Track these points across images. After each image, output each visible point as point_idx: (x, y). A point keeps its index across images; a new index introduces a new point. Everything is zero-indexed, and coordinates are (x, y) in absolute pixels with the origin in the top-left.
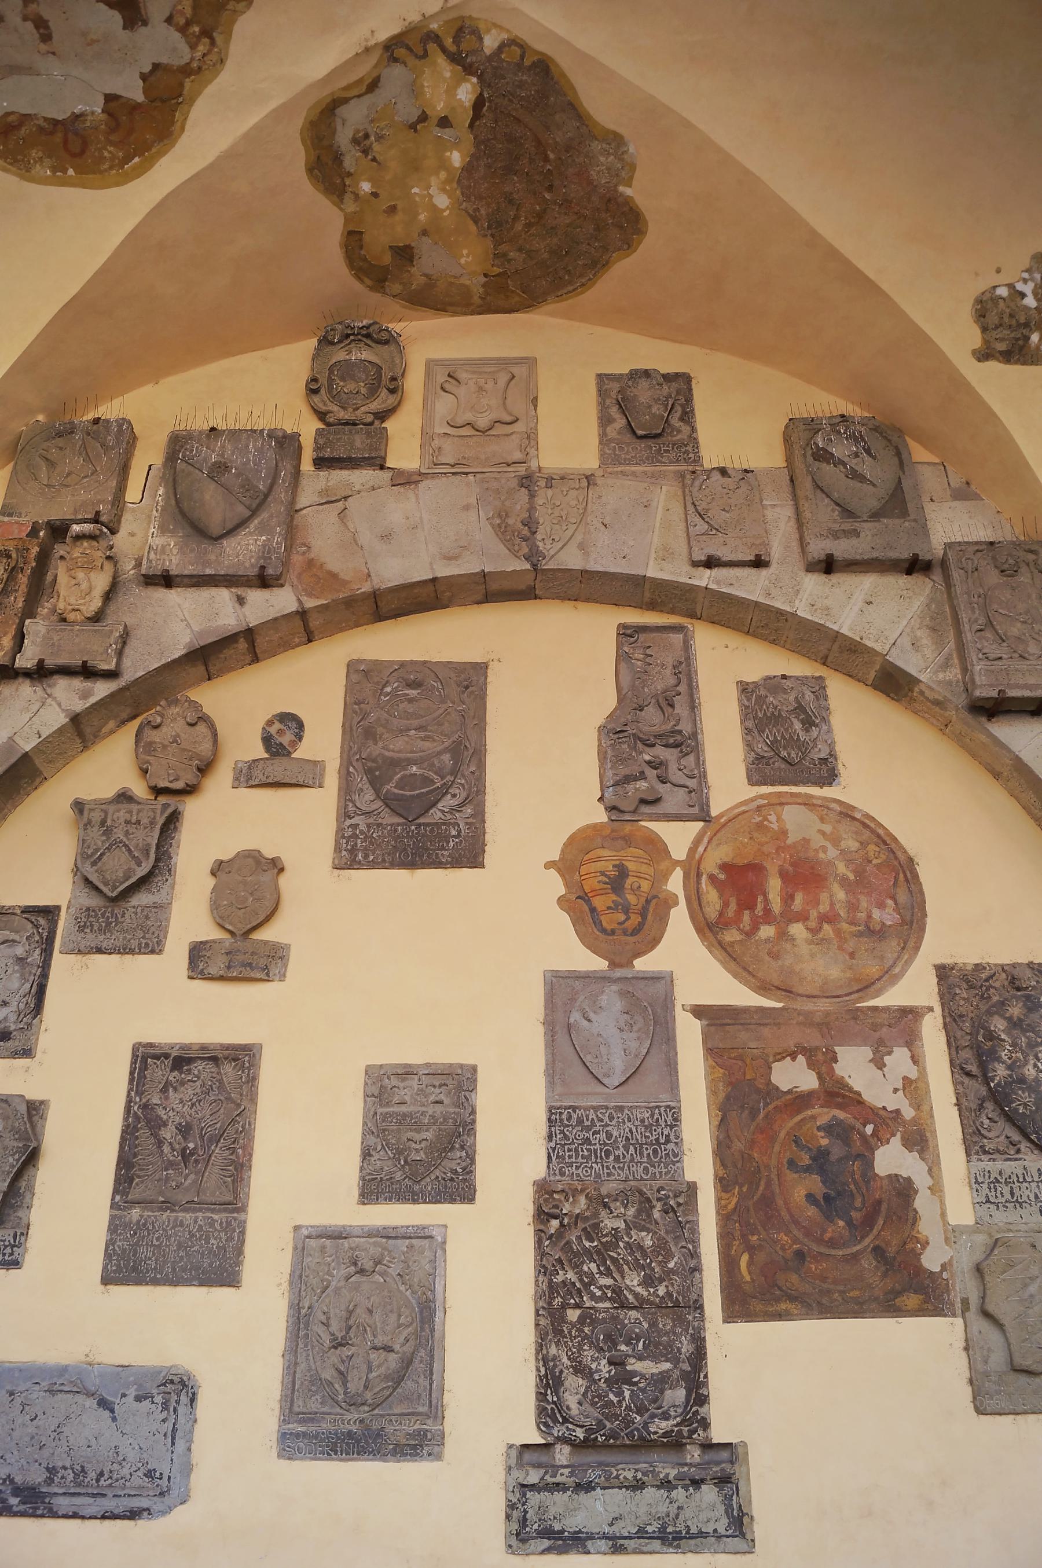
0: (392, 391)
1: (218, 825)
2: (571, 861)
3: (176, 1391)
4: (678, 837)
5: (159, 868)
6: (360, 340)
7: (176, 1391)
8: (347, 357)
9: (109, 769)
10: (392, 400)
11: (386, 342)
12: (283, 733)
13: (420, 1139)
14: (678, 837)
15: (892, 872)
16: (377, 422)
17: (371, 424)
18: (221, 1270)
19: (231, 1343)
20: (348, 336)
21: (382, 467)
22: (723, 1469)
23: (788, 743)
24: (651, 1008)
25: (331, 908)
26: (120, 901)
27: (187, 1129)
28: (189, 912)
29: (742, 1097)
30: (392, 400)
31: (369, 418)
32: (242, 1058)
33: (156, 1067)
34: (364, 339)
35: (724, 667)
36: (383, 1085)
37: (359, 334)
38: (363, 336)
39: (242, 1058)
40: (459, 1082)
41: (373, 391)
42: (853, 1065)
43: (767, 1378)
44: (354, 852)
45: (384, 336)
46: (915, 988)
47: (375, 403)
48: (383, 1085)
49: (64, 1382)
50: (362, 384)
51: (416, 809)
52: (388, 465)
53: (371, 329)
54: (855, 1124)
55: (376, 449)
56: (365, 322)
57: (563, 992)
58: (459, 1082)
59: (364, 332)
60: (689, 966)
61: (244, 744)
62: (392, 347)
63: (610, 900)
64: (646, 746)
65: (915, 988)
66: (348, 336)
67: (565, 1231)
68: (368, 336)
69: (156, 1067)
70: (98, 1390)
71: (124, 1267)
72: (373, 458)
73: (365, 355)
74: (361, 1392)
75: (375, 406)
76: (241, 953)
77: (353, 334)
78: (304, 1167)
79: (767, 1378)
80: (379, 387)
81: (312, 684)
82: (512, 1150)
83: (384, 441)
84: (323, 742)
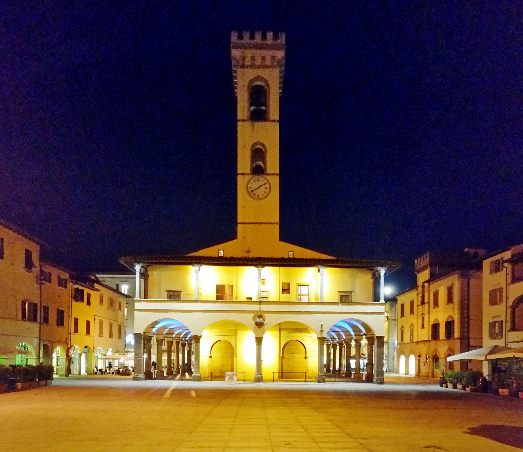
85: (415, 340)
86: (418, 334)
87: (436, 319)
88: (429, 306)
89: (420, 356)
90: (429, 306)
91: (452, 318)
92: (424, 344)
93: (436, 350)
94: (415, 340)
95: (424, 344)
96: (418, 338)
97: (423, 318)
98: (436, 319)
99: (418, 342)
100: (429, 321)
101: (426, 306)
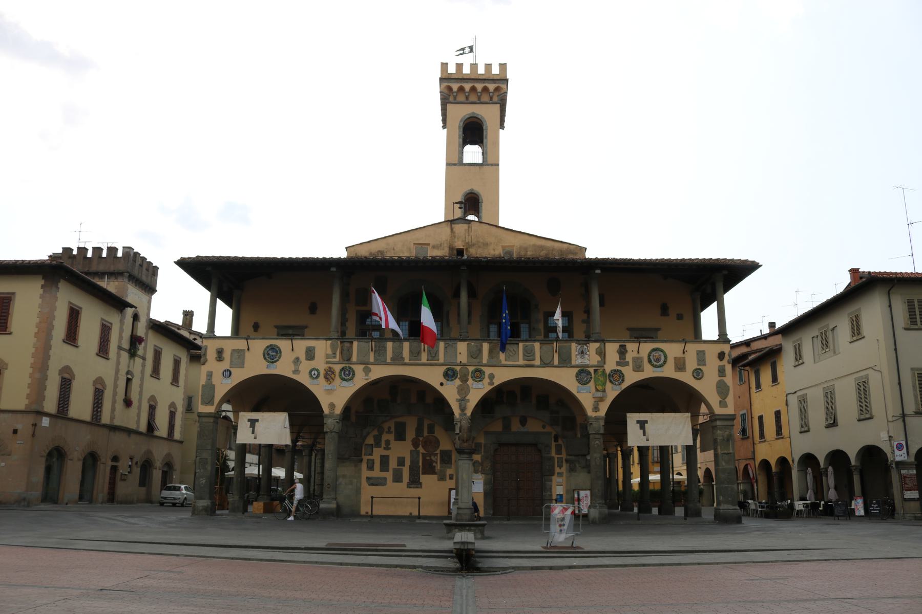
1: (385, 437)
2: (413, 441)
3: (385, 479)
4: (421, 439)
5: (380, 440)
7: (385, 479)
9: (375, 432)
12: (389, 428)
13: (401, 462)
14: (421, 439)
15: (437, 442)
18: (388, 470)
19: (389, 475)
22: (421, 484)
23: (431, 429)
24: (418, 452)
25: (394, 444)
26: (378, 444)
27: (385, 461)
28: (383, 445)
29: (424, 459)
32: (388, 456)
33: (382, 457)
35: (426, 423)
36: (399, 458)
39: (388, 456)
40: (404, 458)
42: (433, 458)
43: (424, 478)
44: (396, 439)
46: (438, 452)
48: (399, 458)
49: (378, 478)
51: (400, 437)
54: (432, 461)
57: (412, 451)
58: (404, 458)
60: (421, 450)
61: (386, 430)
63: (415, 444)
64: (419, 431)
65: (438, 452)
67: (411, 468)
69: (382, 457)
70: (381, 478)
71: (381, 470)
74: (398, 478)
76: (387, 448)
78: (393, 464)
79: (424, 478)
81: (391, 424)
82: (408, 463)
84: (393, 429)
85: (105, 419)
86: (113, 410)
87: (153, 398)
88: (144, 366)
89: (115, 459)
90: (144, 366)
91: (176, 408)
92: (129, 436)
93: (149, 452)
94: (105, 419)
95: (129, 436)
96: (112, 418)
97: (128, 380)
98: (153, 398)
99: (113, 428)
100: (141, 393)
101: (138, 361)
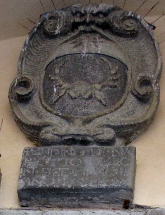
0: (143, 99)
6: (94, 32)
8: (76, 50)
10: (140, 113)
11: (133, 35)
16: (119, 142)
17: (110, 142)
20: (75, 26)
21: (127, 205)
30: (140, 113)
31: (109, 134)
34: (101, 31)
37: (92, 23)
38: (98, 25)
41: (115, 97)
45: (130, 25)
47: (117, 114)
50: (98, 86)
52: (139, 199)
53: (110, 17)
55: (119, 177)
56: (102, 7)
59: (100, 20)
62: (142, 42)
66: (75, 26)
68: (106, 26)
72: (114, 190)
73: (103, 47)
75: (118, 117)
77: (84, 23)
80: (123, 91)
83: (131, 169)
